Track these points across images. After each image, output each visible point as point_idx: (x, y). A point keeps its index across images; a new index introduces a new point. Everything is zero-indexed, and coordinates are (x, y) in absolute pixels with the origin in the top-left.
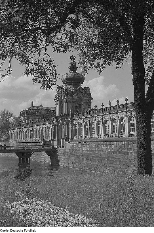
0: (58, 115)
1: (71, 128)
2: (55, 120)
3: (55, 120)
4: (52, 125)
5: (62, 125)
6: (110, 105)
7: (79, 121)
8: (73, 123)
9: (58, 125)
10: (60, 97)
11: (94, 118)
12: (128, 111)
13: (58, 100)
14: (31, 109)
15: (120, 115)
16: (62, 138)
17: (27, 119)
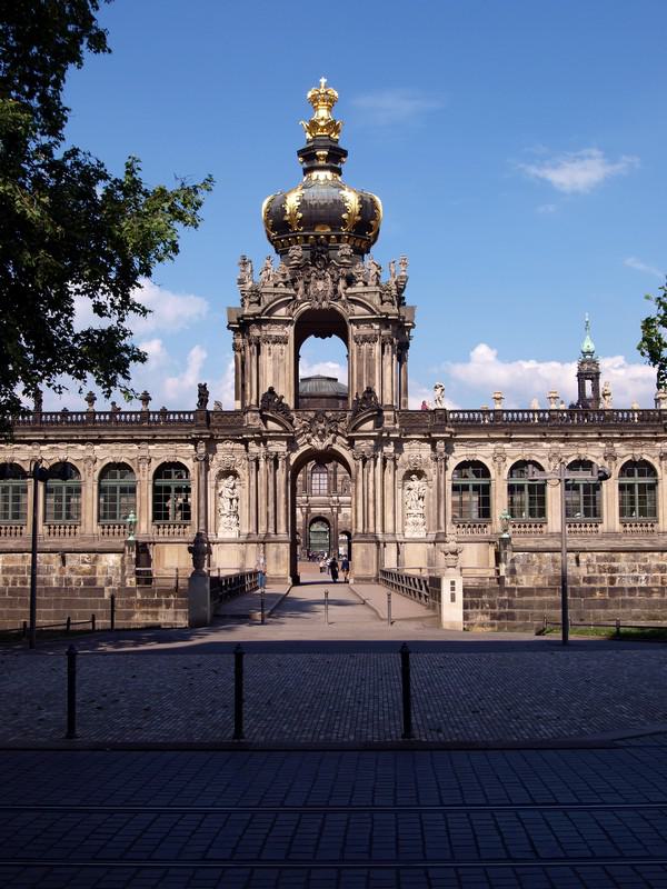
10: (304, 307)
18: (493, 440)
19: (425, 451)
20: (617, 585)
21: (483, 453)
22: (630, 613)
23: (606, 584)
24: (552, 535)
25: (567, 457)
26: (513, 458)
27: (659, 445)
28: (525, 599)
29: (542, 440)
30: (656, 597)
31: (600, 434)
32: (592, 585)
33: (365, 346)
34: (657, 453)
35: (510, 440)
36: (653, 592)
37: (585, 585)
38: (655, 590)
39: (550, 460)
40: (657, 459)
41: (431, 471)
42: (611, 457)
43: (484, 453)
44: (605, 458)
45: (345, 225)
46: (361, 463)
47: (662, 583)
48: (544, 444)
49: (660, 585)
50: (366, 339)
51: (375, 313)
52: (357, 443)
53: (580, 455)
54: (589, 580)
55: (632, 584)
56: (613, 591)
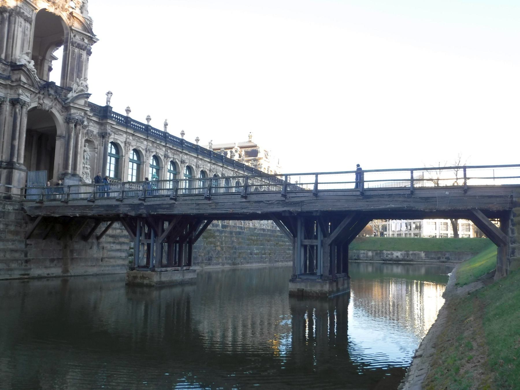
18: (126, 133)
19: (95, 129)
21: (121, 140)
25: (152, 152)
26: (132, 146)
27: (181, 155)
29: (145, 139)
31: (166, 144)
33: (77, 50)
34: (180, 159)
35: (133, 135)
39: (146, 151)
40: (180, 162)
41: (96, 143)
42: (166, 156)
43: (121, 139)
44: (165, 157)
46: (73, 125)
48: (145, 143)
50: (79, 47)
51: (89, 33)
52: (73, 111)
53: (157, 153)
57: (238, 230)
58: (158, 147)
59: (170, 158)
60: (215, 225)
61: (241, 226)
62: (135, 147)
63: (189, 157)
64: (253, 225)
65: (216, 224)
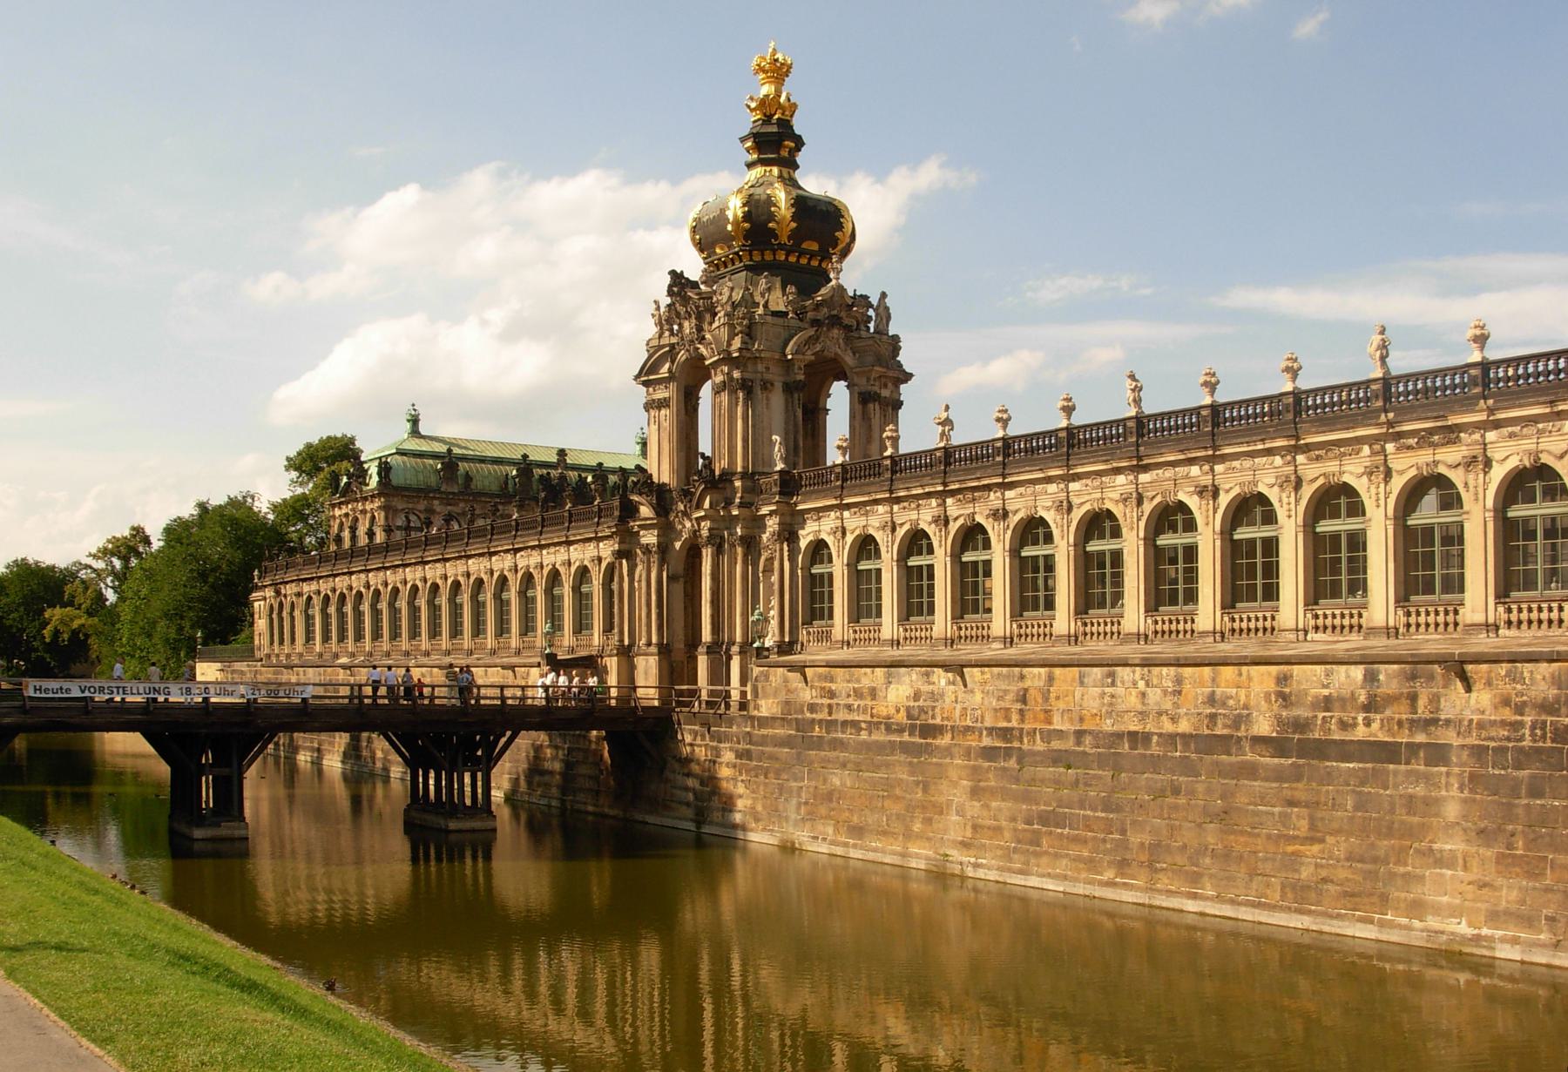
0: (665, 479)
1: (780, 567)
2: (645, 511)
3: (645, 511)
4: (607, 549)
5: (707, 555)
6: (1137, 402)
7: (855, 523)
8: (789, 534)
9: (664, 549)
10: (682, 356)
11: (994, 499)
12: (1307, 448)
13: (671, 377)
14: (401, 453)
15: (907, 517)
16: (706, 635)
17: (380, 517)
20: (833, 717)
22: (838, 758)
23: (823, 715)
24: (1473, 627)
28: (764, 731)
30: (864, 736)
32: (814, 716)
36: (861, 729)
37: (808, 715)
38: (863, 725)
45: (733, 238)
47: (872, 716)
49: (869, 719)
54: (813, 708)
55: (841, 715)
56: (830, 725)
57: (987, 741)
58: (913, 505)
59: (956, 519)
60: (894, 727)
61: (1005, 724)
62: (857, 532)
63: (1021, 490)
64: (1071, 720)
65: (897, 724)
